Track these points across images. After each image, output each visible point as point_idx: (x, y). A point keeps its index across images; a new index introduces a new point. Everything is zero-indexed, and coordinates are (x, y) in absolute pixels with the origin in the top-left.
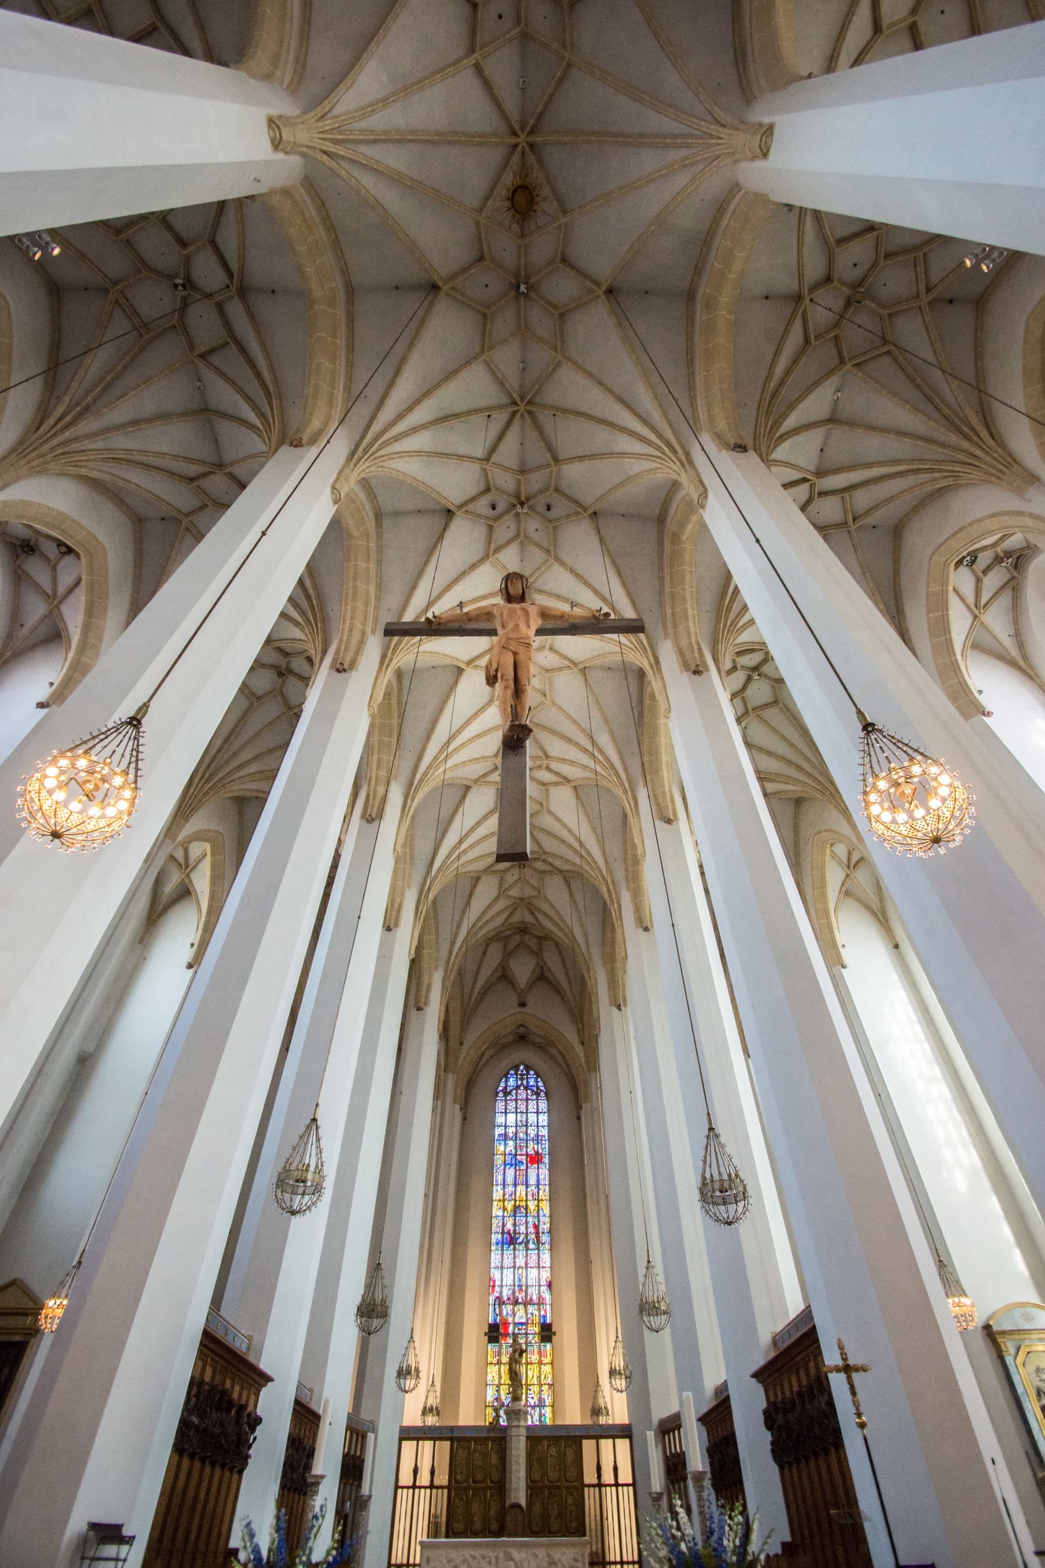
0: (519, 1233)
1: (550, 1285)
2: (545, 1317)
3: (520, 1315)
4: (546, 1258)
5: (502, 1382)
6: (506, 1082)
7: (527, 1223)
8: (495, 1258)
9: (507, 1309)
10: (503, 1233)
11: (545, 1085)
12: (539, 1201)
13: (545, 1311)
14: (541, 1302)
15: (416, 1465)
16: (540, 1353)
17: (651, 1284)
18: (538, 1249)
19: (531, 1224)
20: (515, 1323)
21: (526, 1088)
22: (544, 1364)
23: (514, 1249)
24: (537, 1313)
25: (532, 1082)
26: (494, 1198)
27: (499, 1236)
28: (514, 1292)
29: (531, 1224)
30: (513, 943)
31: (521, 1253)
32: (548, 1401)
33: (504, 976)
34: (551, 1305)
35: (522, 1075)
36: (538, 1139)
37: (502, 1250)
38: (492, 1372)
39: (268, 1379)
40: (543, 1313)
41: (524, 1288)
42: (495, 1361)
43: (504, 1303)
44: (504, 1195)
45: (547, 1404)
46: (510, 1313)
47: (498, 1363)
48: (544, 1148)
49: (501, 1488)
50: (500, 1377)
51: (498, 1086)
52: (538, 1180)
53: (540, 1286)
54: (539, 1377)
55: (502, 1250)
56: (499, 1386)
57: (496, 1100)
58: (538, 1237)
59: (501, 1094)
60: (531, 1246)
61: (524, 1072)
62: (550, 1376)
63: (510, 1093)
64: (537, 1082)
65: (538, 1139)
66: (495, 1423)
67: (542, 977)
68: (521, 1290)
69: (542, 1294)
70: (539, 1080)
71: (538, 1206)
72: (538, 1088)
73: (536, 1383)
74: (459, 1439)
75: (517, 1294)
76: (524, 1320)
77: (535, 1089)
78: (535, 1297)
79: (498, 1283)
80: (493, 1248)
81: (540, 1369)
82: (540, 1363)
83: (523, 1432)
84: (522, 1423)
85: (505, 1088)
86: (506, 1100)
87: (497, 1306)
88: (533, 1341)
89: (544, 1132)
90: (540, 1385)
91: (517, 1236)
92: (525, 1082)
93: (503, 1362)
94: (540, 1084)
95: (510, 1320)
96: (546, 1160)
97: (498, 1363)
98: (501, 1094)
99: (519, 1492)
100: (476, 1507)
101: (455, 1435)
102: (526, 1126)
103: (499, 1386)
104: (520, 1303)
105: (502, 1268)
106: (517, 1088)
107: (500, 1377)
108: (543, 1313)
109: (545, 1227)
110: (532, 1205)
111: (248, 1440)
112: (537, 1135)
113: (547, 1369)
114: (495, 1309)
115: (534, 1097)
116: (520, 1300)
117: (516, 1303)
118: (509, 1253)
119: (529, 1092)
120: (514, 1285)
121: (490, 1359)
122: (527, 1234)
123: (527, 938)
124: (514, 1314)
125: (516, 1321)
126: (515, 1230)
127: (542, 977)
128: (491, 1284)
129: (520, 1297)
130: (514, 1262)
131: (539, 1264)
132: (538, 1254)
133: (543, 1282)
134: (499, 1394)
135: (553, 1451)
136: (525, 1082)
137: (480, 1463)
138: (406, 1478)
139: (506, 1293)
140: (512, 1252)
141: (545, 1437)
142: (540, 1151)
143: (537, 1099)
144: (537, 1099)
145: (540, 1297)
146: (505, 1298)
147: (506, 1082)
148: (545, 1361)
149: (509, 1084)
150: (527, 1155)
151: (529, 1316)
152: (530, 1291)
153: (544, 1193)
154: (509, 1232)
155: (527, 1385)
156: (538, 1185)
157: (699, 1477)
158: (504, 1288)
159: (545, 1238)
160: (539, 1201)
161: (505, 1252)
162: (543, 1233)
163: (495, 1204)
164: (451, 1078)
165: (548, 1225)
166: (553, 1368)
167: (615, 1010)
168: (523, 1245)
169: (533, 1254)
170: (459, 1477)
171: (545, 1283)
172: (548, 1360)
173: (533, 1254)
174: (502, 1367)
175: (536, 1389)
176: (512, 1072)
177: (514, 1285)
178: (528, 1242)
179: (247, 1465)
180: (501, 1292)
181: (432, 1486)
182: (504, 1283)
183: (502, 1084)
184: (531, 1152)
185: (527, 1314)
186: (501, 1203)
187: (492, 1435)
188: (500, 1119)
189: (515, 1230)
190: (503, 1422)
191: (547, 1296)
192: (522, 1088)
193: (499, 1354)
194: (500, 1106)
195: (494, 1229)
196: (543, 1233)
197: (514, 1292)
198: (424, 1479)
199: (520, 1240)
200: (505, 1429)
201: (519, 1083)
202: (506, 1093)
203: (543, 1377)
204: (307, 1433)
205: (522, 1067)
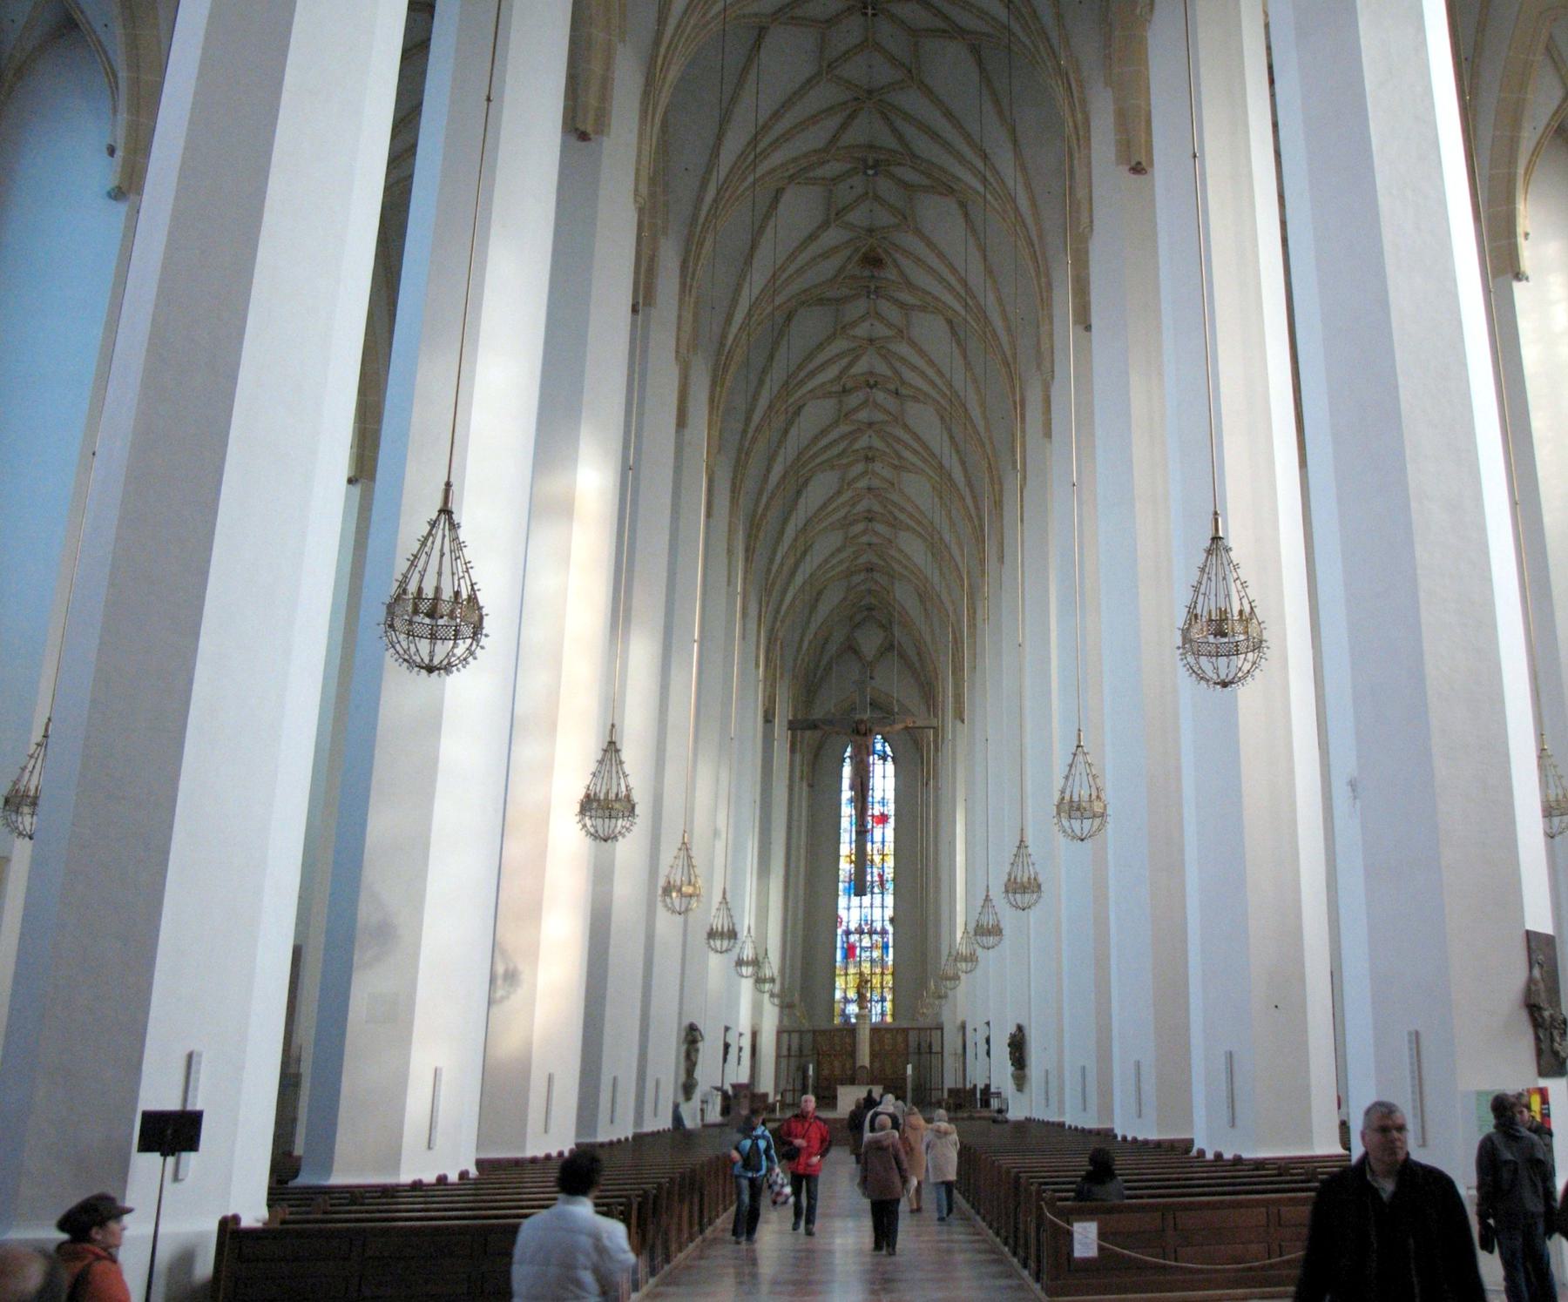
1: (892, 920)
3: (866, 942)
4: (889, 900)
7: (872, 873)
8: (842, 901)
9: (853, 938)
12: (883, 855)
14: (884, 932)
16: (883, 969)
17: (1020, 865)
18: (883, 893)
19: (876, 874)
24: (880, 940)
25: (879, 747)
27: (847, 885)
29: (876, 874)
30: (858, 618)
31: (866, 899)
33: (851, 648)
34: (894, 934)
36: (883, 802)
38: (840, 982)
42: (842, 973)
48: (890, 810)
49: (852, 1054)
50: (846, 983)
51: (845, 751)
52: (883, 838)
53: (883, 921)
57: (843, 766)
60: (876, 890)
64: (884, 747)
65: (883, 802)
67: (889, 647)
68: (866, 924)
70: (887, 744)
71: (883, 860)
72: (885, 752)
76: (869, 945)
77: (881, 753)
78: (879, 929)
79: (845, 919)
80: (840, 893)
82: (882, 974)
89: (890, 795)
90: (882, 988)
94: (888, 749)
95: (858, 944)
96: (892, 820)
99: (864, 1057)
100: (836, 1063)
105: (849, 909)
109: (889, 874)
110: (877, 859)
112: (883, 799)
113: (889, 979)
115: (881, 761)
119: (876, 756)
121: (838, 972)
122: (872, 882)
123: (874, 613)
124: (861, 940)
127: (889, 647)
133: (887, 918)
139: (853, 927)
142: (886, 812)
148: (886, 972)
150: (873, 816)
152: (874, 924)
153: (890, 848)
156: (883, 842)
159: (890, 886)
160: (883, 855)
164: (798, 757)
165: (892, 875)
167: (958, 723)
169: (878, 898)
172: (890, 970)
173: (878, 898)
175: (879, 990)
190: (853, 1020)
191: (890, 929)
193: (846, 969)
195: (841, 878)
197: (860, 925)
200: (855, 1024)
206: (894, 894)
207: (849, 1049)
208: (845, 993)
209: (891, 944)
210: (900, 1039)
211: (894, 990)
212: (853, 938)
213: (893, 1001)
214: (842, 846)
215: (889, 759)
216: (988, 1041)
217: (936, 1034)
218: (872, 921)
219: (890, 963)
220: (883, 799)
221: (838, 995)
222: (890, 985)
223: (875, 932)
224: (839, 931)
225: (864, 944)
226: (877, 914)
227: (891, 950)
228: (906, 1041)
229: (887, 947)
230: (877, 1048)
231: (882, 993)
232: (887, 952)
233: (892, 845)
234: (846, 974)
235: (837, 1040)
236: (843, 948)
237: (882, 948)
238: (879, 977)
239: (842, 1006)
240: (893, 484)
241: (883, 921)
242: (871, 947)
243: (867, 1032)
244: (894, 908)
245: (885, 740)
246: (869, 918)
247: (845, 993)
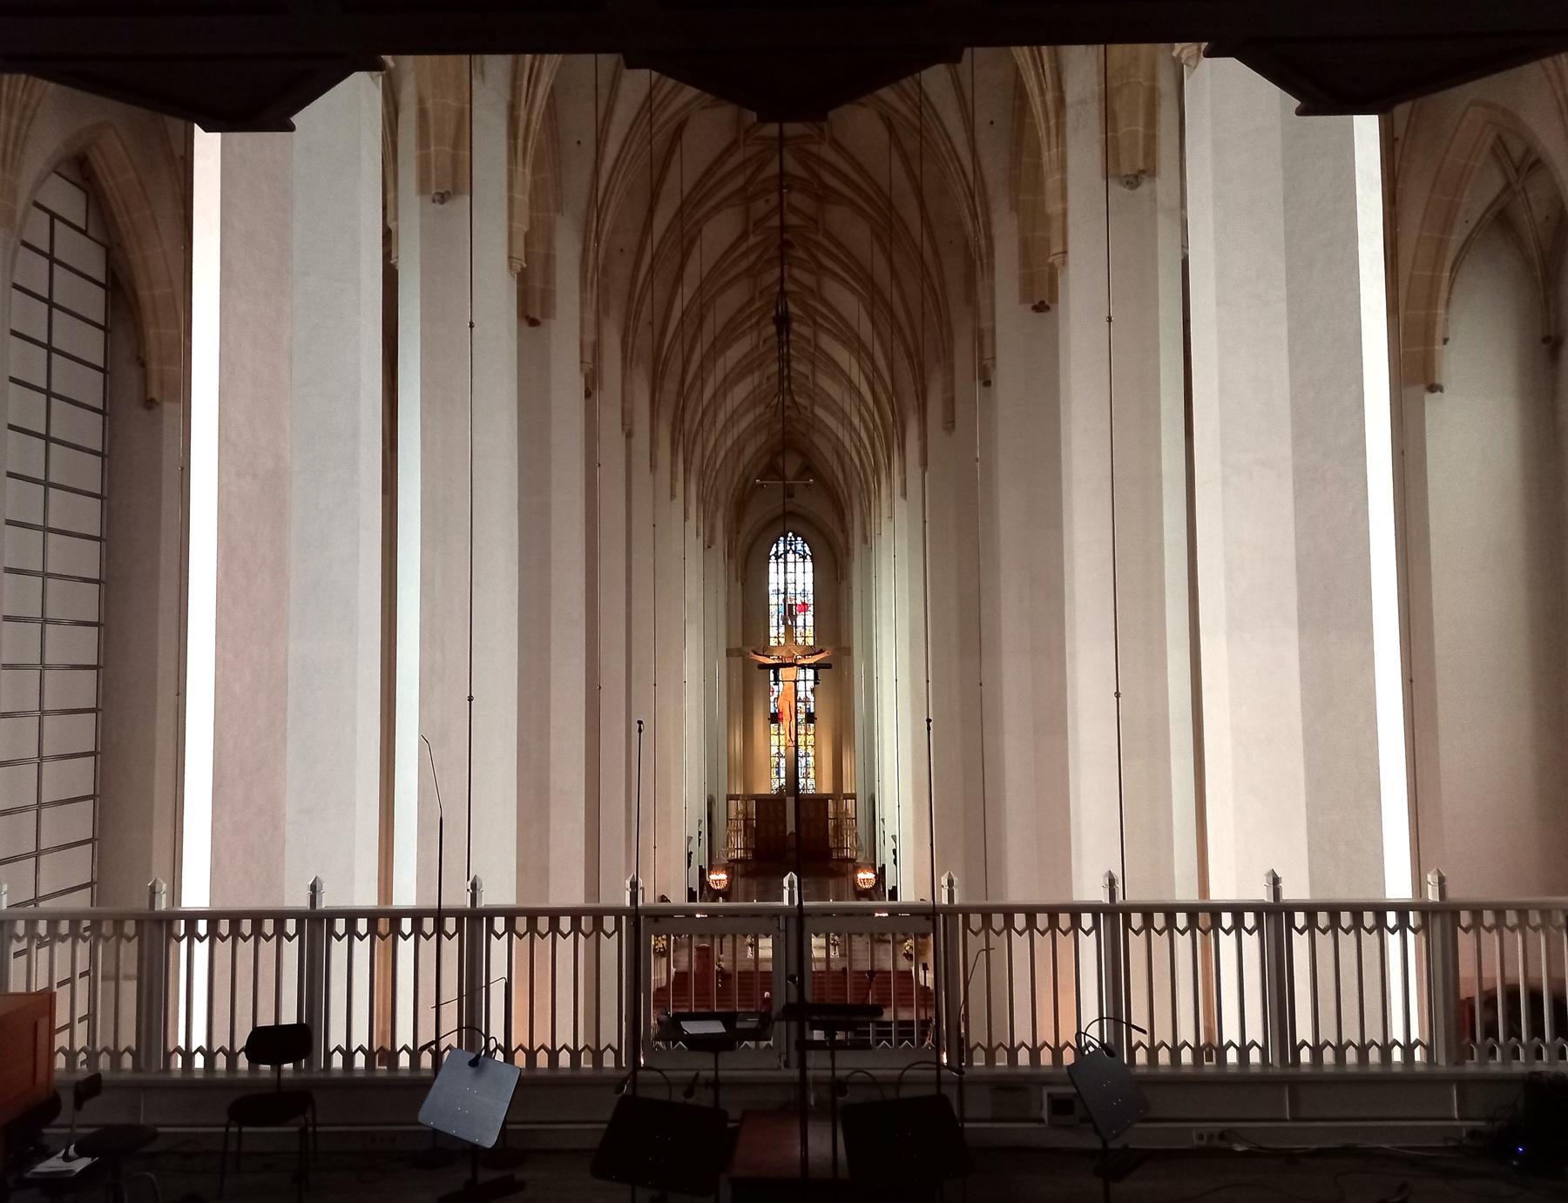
2: (809, 709)
6: (777, 547)
11: (810, 550)
14: (806, 701)
16: (806, 730)
21: (795, 552)
26: (771, 635)
32: (812, 754)
35: (791, 541)
38: (774, 740)
40: (808, 707)
44: (778, 633)
48: (810, 599)
53: (806, 691)
54: (805, 742)
59: (773, 558)
61: (793, 539)
63: (780, 557)
64: (804, 547)
70: (806, 545)
71: (805, 641)
72: (804, 551)
74: (760, 800)
77: (802, 553)
82: (806, 734)
85: (777, 552)
86: (777, 563)
89: (810, 588)
90: (806, 745)
92: (793, 547)
94: (807, 549)
96: (811, 608)
98: (773, 558)
102: (795, 583)
106: (786, 552)
115: (802, 560)
119: (797, 555)
133: (808, 688)
136: (793, 547)
142: (806, 602)
143: (804, 562)
144: (804, 562)
147: (777, 547)
149: (779, 549)
160: (805, 637)
163: (771, 639)
172: (812, 732)
176: (782, 538)
183: (774, 549)
184: (799, 602)
186: (776, 640)
188: (773, 577)
191: (812, 698)
192: (791, 552)
194: (772, 567)
201: (788, 548)
202: (777, 557)
205: (790, 534)
214: (771, 628)
215: (808, 557)
216: (895, 851)
220: (804, 590)
221: (774, 750)
224: (772, 699)
231: (806, 750)
233: (812, 628)
234: (779, 734)
239: (777, 759)
240: (808, 378)
245: (805, 541)
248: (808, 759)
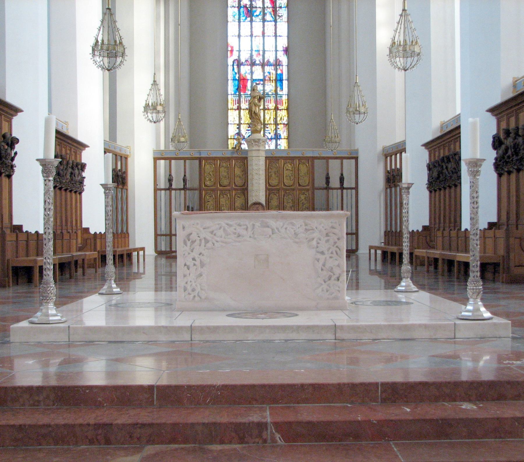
0: (256, 7)
1: (286, 51)
3: (258, 73)
4: (283, 27)
5: (242, 122)
8: (232, 28)
10: (239, 7)
13: (282, 71)
14: (277, 64)
15: (170, 175)
16: (276, 102)
18: (275, 21)
20: (254, 80)
22: (280, 110)
23: (251, 21)
24: (274, 72)
27: (236, 10)
28: (251, 56)
31: (258, 25)
34: (288, 66)
37: (239, 22)
38: (233, 116)
39: (16, 111)
40: (279, 72)
41: (261, 53)
42: (235, 107)
43: (242, 64)
45: (282, 137)
46: (249, 71)
47: (238, 109)
50: (240, 118)
53: (276, 51)
54: (276, 119)
55: (239, 22)
56: (239, 125)
58: (275, 11)
60: (268, 17)
62: (286, 118)
66: (237, 148)
69: (278, 57)
73: (273, 123)
75: (255, 57)
76: (262, 78)
78: (272, 60)
79: (236, 48)
81: (276, 114)
82: (276, 109)
83: (263, 154)
84: (261, 148)
87: (235, 67)
88: (270, 93)
90: (276, 124)
91: (254, 9)
93: (242, 108)
95: (249, 77)
97: (238, 109)
101: (203, 155)
103: (239, 125)
104: (258, 65)
105: (239, 36)
107: (240, 118)
108: (279, 72)
111: (10, 155)
113: (283, 114)
114: (233, 70)
116: (258, 62)
117: (253, 64)
118: (246, 25)
120: (252, 50)
121: (230, 106)
122: (264, 8)
124: (252, 73)
125: (254, 78)
126: (251, 5)
128: (229, 49)
129: (258, 59)
130: (252, 32)
131: (276, 33)
132: (276, 25)
133: (280, 48)
134: (240, 130)
135: (289, 166)
137: (225, 174)
138: (163, 184)
140: (249, 23)
141: (282, 158)
145: (276, 59)
146: (243, 60)
148: (280, 107)
151: (266, 74)
154: (245, 6)
155: (265, 125)
157: (476, 164)
158: (241, 53)
159: (283, 12)
161: (242, 23)
162: (281, 7)
166: (288, 114)
168: (260, 17)
169: (269, 26)
170: (208, 183)
171: (282, 49)
172: (285, 106)
173: (269, 26)
174: (242, 111)
175: (273, 127)
177: (252, 50)
178: (264, 14)
179: (13, 171)
180: (239, 56)
181: (185, 189)
182: (241, 49)
185: (264, 72)
187: (235, 155)
189: (251, 5)
190: (245, 146)
191: (284, 59)
193: (239, 102)
196: (281, 7)
197: (251, 56)
198: (177, 183)
199: (257, 13)
200: (246, 151)
203: (279, 119)
204: (68, 152)
206: (288, 22)
207: (239, 182)
208: (239, 128)
209: (285, 77)
210: (303, 169)
211: (288, 125)
212: (245, 70)
213: (288, 138)
217: (349, 165)
218: (264, 51)
219: (285, 98)
221: (232, 131)
222: (285, 121)
223: (269, 64)
224: (230, 61)
225: (255, 77)
226: (270, 42)
227: (285, 83)
228: (311, 172)
229: (281, 80)
230: (274, 182)
231: (276, 129)
232: (282, 86)
234: (239, 108)
235: (223, 172)
236: (234, 80)
237: (276, 80)
238: (273, 113)
241: (276, 51)
242: (264, 80)
243: (262, 162)
244: (288, 37)
246: (261, 49)
247: (239, 128)
248: (279, 142)
